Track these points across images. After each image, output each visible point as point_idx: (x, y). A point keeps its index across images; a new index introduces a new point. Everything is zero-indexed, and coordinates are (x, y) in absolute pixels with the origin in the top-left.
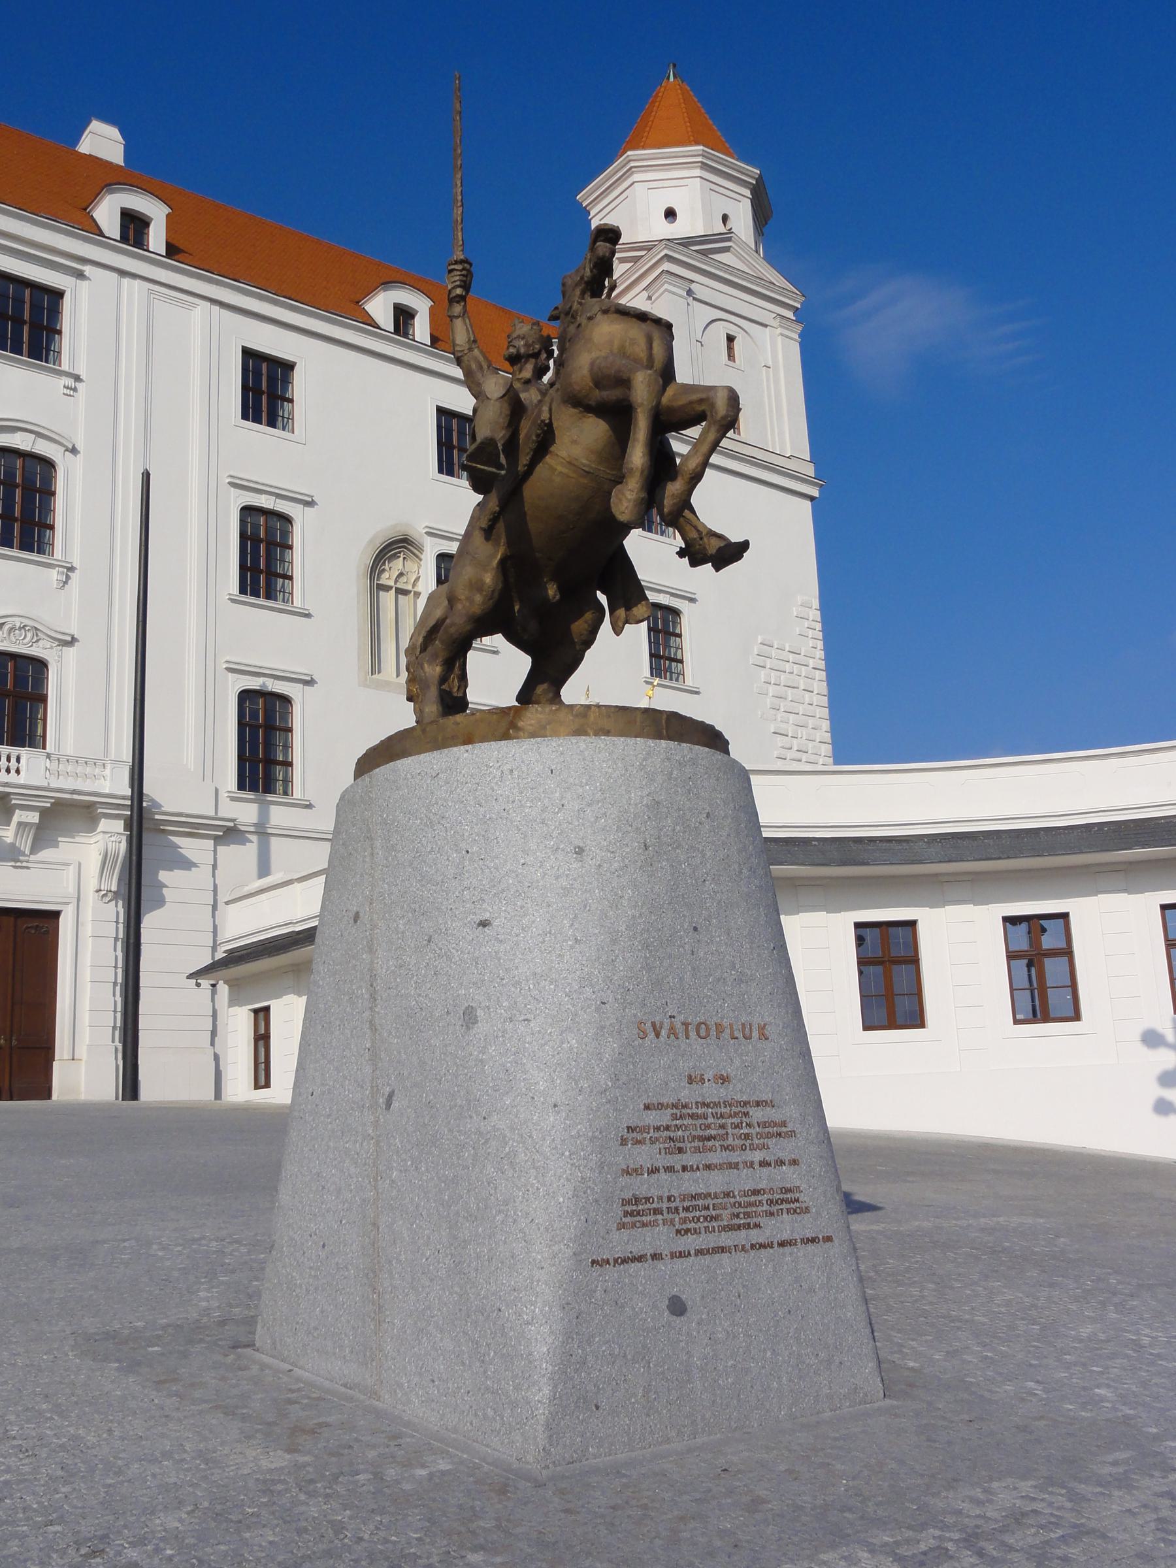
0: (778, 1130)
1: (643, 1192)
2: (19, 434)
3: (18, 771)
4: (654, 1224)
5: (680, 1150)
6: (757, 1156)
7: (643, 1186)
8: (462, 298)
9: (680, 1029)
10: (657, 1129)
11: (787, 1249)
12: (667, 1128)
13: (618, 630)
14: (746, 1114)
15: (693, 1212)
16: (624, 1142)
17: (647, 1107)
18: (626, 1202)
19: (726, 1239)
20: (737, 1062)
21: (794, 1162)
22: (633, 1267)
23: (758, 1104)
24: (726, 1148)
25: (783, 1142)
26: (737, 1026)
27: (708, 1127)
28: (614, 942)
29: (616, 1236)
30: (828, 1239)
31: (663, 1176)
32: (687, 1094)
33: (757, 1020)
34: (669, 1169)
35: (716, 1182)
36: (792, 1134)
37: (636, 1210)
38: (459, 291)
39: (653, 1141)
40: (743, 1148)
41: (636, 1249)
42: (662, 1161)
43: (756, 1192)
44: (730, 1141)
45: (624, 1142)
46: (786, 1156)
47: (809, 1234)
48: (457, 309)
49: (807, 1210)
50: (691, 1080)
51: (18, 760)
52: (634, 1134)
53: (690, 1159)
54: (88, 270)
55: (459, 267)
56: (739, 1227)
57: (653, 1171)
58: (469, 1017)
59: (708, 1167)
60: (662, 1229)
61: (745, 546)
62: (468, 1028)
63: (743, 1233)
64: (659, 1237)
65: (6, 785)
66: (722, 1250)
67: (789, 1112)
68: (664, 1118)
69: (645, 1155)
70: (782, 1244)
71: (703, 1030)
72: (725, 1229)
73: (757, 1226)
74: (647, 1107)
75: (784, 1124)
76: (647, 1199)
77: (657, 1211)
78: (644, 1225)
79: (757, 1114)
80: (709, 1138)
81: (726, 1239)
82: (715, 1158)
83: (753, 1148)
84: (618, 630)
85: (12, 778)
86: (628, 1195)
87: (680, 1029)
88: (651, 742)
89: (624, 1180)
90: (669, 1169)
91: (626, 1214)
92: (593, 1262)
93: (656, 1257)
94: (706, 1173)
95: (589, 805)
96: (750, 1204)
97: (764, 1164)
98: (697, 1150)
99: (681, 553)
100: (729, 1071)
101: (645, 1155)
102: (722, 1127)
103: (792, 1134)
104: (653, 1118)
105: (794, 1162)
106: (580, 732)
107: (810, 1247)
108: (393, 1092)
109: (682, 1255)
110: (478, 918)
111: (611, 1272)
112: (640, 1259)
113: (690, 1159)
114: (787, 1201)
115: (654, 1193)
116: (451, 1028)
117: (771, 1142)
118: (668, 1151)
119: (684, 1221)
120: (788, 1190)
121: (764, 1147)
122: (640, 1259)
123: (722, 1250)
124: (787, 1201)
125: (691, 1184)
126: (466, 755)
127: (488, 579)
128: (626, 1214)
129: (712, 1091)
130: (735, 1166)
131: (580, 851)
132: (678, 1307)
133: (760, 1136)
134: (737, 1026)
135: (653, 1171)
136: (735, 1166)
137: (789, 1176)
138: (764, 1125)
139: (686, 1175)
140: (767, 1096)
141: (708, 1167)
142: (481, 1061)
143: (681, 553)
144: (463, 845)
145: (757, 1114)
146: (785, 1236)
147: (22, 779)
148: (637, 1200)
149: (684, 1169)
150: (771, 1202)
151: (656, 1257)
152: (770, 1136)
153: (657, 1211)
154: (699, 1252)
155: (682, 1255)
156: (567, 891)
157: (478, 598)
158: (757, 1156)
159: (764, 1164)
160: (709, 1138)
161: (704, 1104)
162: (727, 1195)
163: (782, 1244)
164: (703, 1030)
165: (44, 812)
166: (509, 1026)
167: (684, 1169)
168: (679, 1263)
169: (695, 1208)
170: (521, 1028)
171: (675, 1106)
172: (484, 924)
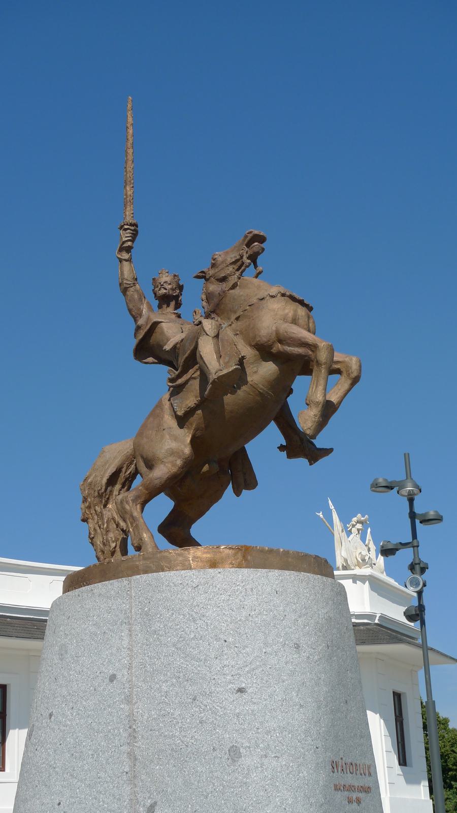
8: (129, 250)
13: (238, 493)
28: (319, 708)
38: (129, 243)
48: (125, 256)
55: (132, 228)
58: (234, 753)
61: (331, 450)
62: (234, 761)
84: (238, 493)
95: (300, 617)
99: (282, 448)
106: (285, 566)
108: (155, 803)
110: (236, 686)
116: (217, 761)
126: (219, 575)
127: (187, 450)
131: (297, 647)
142: (245, 783)
143: (282, 448)
144: (222, 636)
156: (292, 673)
157: (179, 462)
166: (266, 761)
172: (241, 690)
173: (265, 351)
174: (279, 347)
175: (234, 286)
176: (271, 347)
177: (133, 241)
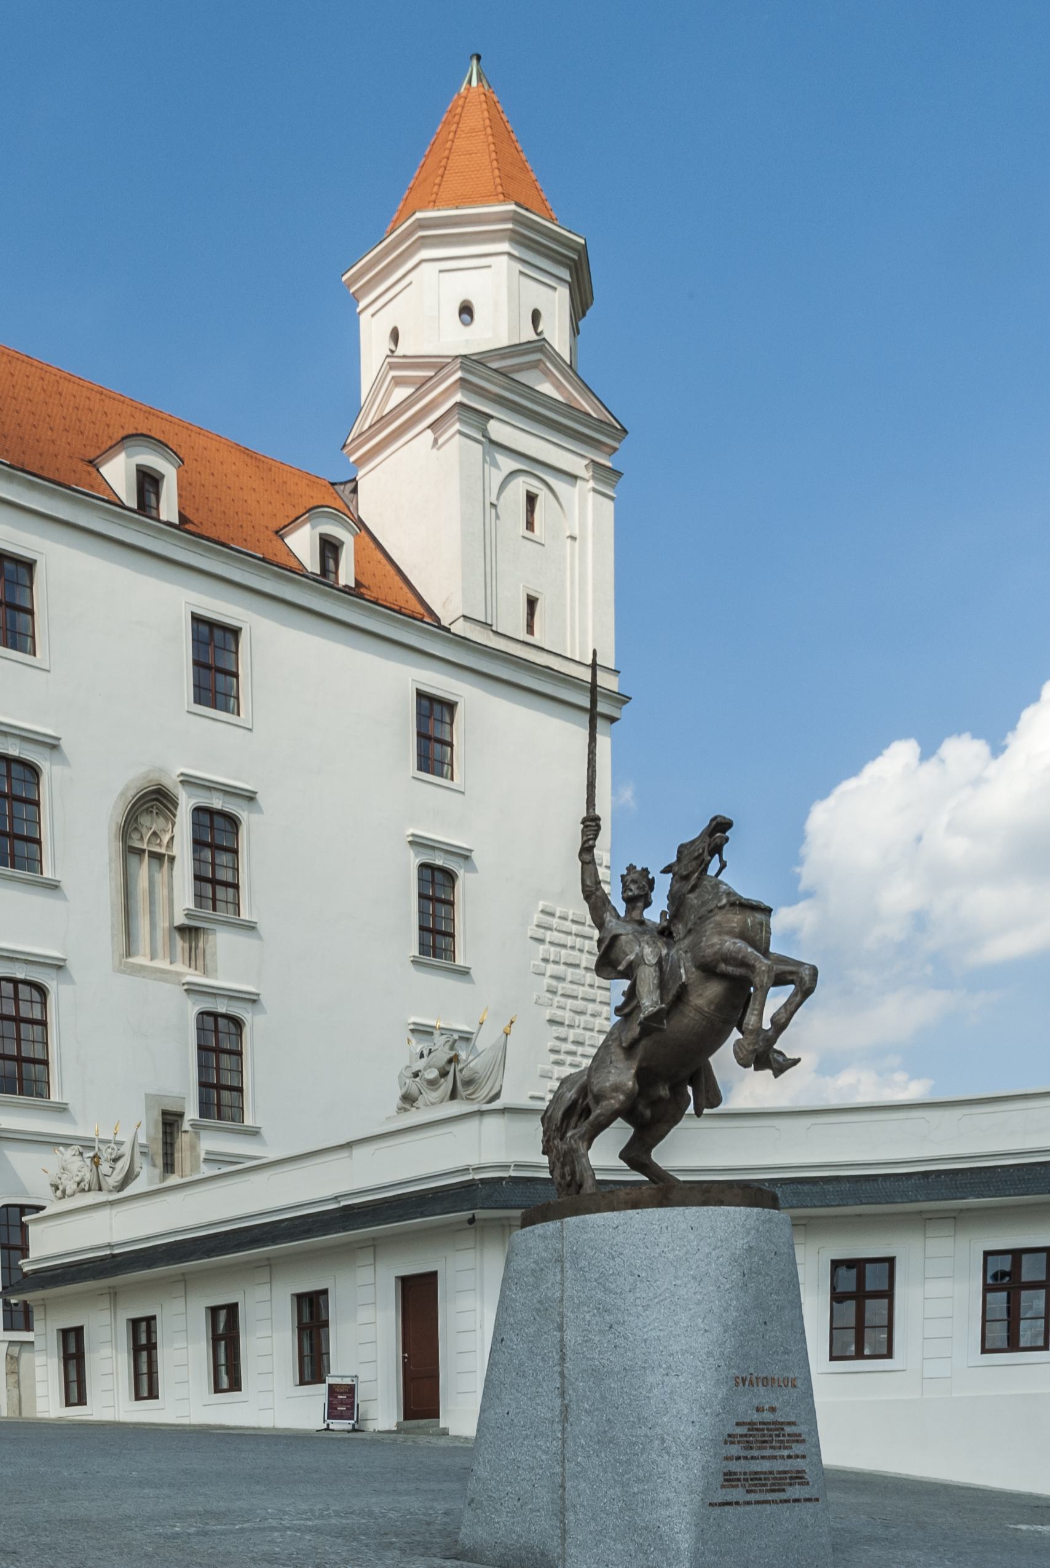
0: (798, 1439)
1: (733, 1469)
4: (737, 1486)
5: (751, 1448)
6: (786, 1453)
7: (734, 1466)
9: (754, 1380)
10: (741, 1436)
11: (797, 1504)
12: (746, 1436)
14: (783, 1429)
15: (755, 1480)
16: (726, 1442)
17: (738, 1424)
18: (725, 1474)
19: (770, 1497)
20: (780, 1400)
21: (804, 1457)
22: (727, 1508)
23: (790, 1424)
24: (771, 1447)
25: (799, 1445)
26: (781, 1379)
27: (764, 1436)
28: (726, 1331)
29: (720, 1491)
30: (817, 1500)
31: (742, 1461)
32: (756, 1417)
33: (791, 1376)
34: (746, 1458)
35: (766, 1466)
36: (804, 1441)
37: (730, 1479)
39: (739, 1442)
40: (780, 1448)
41: (729, 1498)
42: (742, 1453)
43: (785, 1472)
44: (774, 1444)
46: (799, 1453)
47: (807, 1496)
50: (758, 1410)
52: (731, 1439)
53: (756, 1453)
57: (738, 1458)
59: (763, 1458)
60: (740, 1489)
63: (777, 1494)
64: (737, 1494)
67: (802, 1429)
69: (735, 1450)
71: (766, 1382)
72: (767, 1491)
73: (784, 1490)
74: (738, 1424)
75: (800, 1435)
76: (735, 1473)
77: (739, 1480)
78: (733, 1486)
79: (788, 1429)
80: (765, 1442)
81: (770, 1497)
82: (767, 1453)
83: (786, 1448)
86: (726, 1471)
87: (754, 1380)
88: (749, 1209)
89: (725, 1463)
90: (746, 1458)
91: (726, 1480)
92: (710, 1504)
93: (737, 1503)
94: (762, 1461)
96: (781, 1479)
97: (789, 1457)
98: (759, 1448)
100: (776, 1404)
102: (771, 1436)
103: (804, 1441)
104: (740, 1430)
105: (804, 1457)
107: (808, 1504)
109: (748, 1503)
111: (717, 1510)
112: (729, 1504)
114: (798, 1477)
115: (738, 1470)
117: (793, 1445)
118: (746, 1448)
119: (750, 1485)
121: (790, 1448)
122: (729, 1504)
124: (798, 1477)
128: (726, 1480)
129: (767, 1416)
130: (775, 1457)
133: (788, 1441)
134: (781, 1379)
135: (738, 1458)
136: (775, 1457)
137: (800, 1464)
138: (789, 1435)
139: (752, 1462)
140: (792, 1420)
141: (763, 1458)
145: (788, 1429)
146: (796, 1497)
148: (730, 1473)
149: (752, 1458)
150: (791, 1478)
151: (737, 1503)
152: (794, 1441)
153: (739, 1480)
154: (758, 1502)
155: (748, 1503)
158: (786, 1453)
159: (789, 1457)
160: (765, 1442)
161: (764, 1424)
162: (771, 1473)
164: (766, 1382)
166: (666, 1379)
167: (752, 1458)
168: (748, 1508)
169: (756, 1479)
170: (674, 1380)
171: (750, 1424)
173: (708, 970)
174: (722, 967)
175: (693, 889)
176: (716, 967)
177: (595, 839)
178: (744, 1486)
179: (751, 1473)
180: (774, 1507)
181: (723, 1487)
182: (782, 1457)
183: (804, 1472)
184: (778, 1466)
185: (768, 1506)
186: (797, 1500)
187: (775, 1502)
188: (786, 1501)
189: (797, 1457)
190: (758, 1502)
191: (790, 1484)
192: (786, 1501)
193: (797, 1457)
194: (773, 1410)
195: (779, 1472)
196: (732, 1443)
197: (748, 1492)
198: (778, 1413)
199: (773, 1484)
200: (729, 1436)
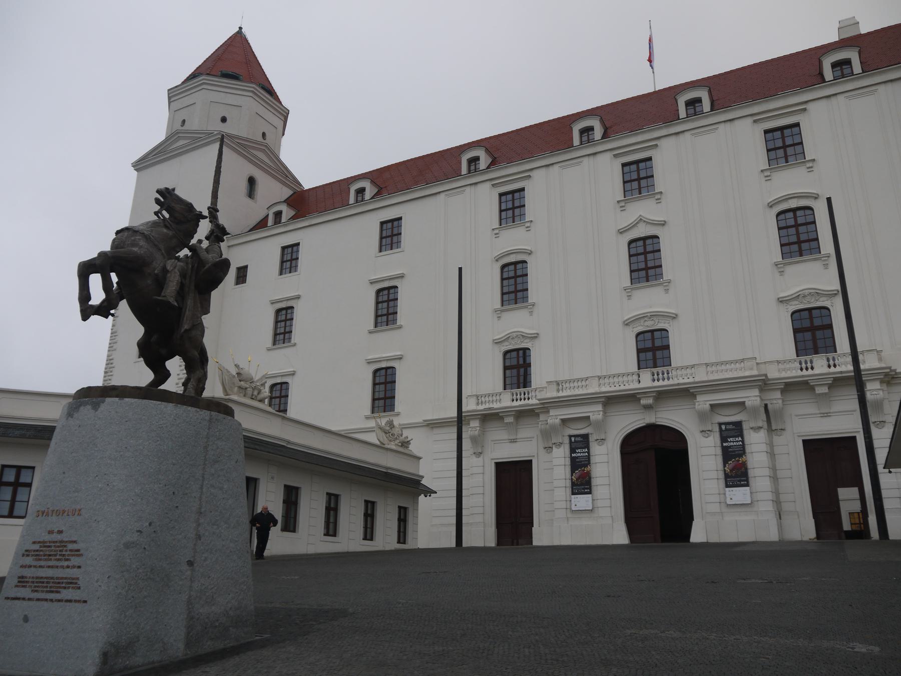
0: (77, 553)
2: (790, 201)
3: (812, 368)
5: (40, 560)
6: (66, 564)
9: (50, 513)
11: (68, 604)
15: (40, 584)
17: (34, 543)
18: (19, 577)
21: (79, 567)
22: (16, 602)
30: (85, 602)
32: (47, 538)
33: (78, 507)
34: (35, 567)
35: (50, 573)
43: (62, 578)
45: (23, 555)
46: (77, 564)
47: (77, 598)
49: (79, 588)
51: (811, 362)
52: (27, 553)
53: (42, 563)
54: (810, 106)
56: (52, 592)
57: (30, 566)
59: (49, 567)
64: (25, 592)
65: (803, 376)
66: (46, 600)
68: (37, 547)
69: (29, 560)
70: (67, 601)
72: (47, 592)
74: (34, 543)
75: (78, 550)
76: (26, 577)
79: (71, 546)
85: (810, 372)
87: (50, 513)
90: (35, 567)
93: (24, 599)
96: (59, 583)
97: (68, 567)
98: (45, 560)
101: (29, 560)
103: (81, 555)
105: (79, 567)
109: (29, 599)
111: (10, 603)
113: (42, 563)
114: (73, 583)
115: (29, 575)
117: (72, 558)
119: (35, 587)
120: (73, 579)
121: (67, 560)
123: (46, 600)
124: (73, 583)
125: (43, 573)
132: (26, 619)
135: (30, 566)
138: (71, 550)
140: (74, 539)
141: (49, 567)
146: (69, 598)
147: (816, 371)
148: (23, 577)
151: (24, 599)
152: (73, 555)
153: (27, 582)
154: (38, 600)
158: (66, 564)
159: (68, 567)
161: (54, 542)
162: (52, 578)
163: (67, 601)
165: (830, 387)
168: (31, 603)
178: (30, 586)
179: (37, 578)
180: (50, 603)
181: (17, 586)
182: (62, 567)
183: (78, 579)
184: (59, 573)
185: (45, 603)
186: (70, 601)
187: (51, 600)
188: (59, 601)
189: (74, 567)
190: (38, 600)
191: (65, 588)
192: (59, 601)
193: (74, 567)
194: (60, 532)
195: (58, 578)
196: (28, 555)
197: (33, 591)
198: (64, 534)
199: (51, 587)
200: (27, 551)
